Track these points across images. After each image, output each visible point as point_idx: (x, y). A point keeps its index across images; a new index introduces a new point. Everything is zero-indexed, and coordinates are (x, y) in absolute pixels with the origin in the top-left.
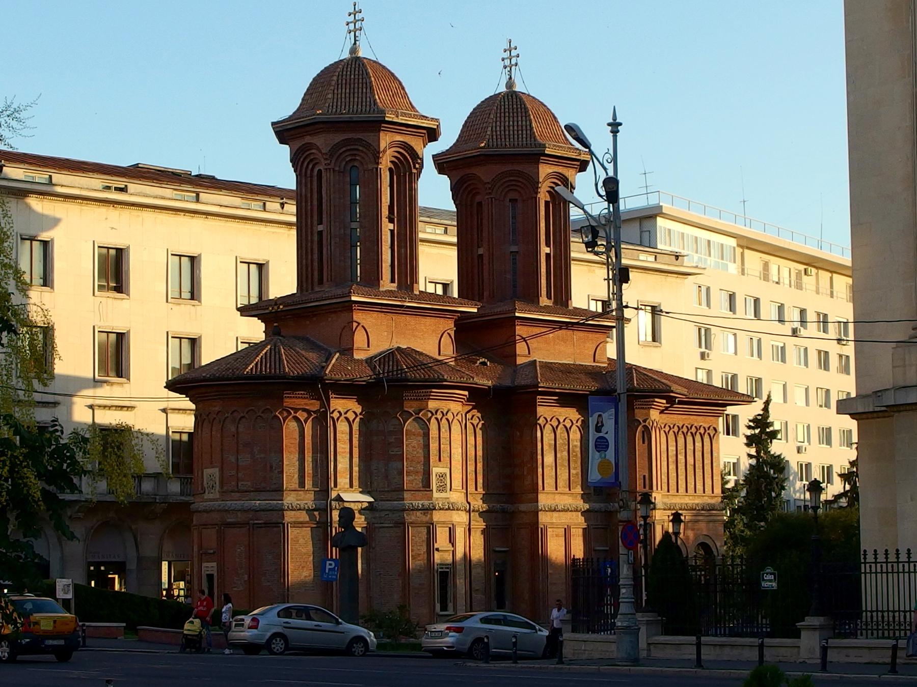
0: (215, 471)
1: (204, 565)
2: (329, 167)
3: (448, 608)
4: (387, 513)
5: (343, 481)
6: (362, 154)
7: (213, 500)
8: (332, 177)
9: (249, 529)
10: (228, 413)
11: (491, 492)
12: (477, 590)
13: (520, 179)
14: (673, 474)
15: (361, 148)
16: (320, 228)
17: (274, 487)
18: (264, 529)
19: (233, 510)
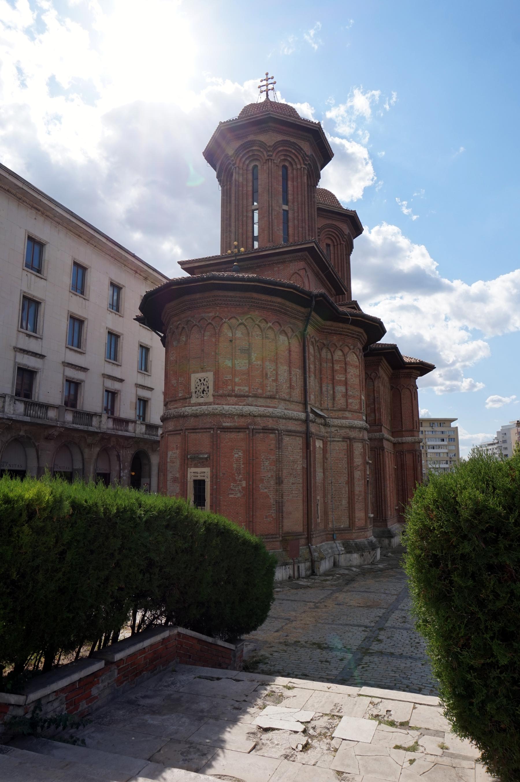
0: (210, 376)
2: (271, 158)
5: (312, 397)
7: (206, 404)
15: (293, 151)
17: (268, 394)
18: (261, 435)
19: (230, 414)
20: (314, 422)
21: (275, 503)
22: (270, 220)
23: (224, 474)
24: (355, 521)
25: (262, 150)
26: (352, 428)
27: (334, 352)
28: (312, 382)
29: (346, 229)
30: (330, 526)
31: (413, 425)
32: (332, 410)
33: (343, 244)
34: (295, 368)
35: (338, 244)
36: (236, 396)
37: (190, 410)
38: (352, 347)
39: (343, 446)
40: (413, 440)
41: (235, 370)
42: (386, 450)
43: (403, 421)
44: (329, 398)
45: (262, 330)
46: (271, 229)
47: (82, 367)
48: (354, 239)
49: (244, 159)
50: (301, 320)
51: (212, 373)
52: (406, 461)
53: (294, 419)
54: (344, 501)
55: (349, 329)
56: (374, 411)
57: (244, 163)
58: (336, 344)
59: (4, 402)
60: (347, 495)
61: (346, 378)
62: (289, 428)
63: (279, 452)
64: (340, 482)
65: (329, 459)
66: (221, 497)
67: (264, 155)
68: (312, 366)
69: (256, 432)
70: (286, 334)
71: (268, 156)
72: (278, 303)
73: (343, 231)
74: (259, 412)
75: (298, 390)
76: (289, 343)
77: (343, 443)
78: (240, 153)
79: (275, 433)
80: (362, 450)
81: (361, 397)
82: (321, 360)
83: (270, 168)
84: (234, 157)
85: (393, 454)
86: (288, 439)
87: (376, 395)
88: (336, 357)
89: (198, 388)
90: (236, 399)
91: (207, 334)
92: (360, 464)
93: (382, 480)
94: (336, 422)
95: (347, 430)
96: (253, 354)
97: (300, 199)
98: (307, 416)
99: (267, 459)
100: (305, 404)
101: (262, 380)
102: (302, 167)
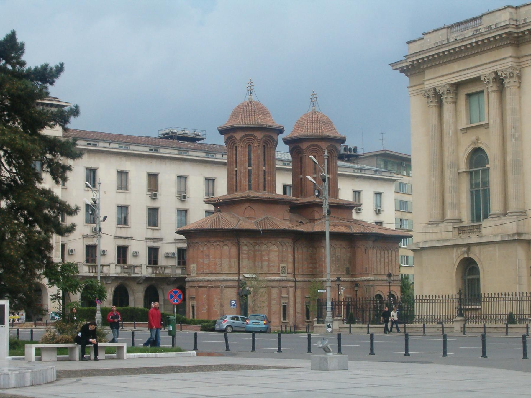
0: (195, 265)
1: (191, 302)
3: (286, 319)
5: (245, 270)
6: (253, 141)
11: (304, 273)
12: (299, 312)
13: (317, 148)
14: (379, 267)
15: (252, 138)
16: (236, 169)
17: (217, 272)
18: (214, 288)
28: (245, 263)
45: (214, 246)
59: (141, 269)
70: (228, 246)
77: (265, 288)
82: (255, 251)
91: (194, 249)
98: (239, 279)
100: (239, 274)
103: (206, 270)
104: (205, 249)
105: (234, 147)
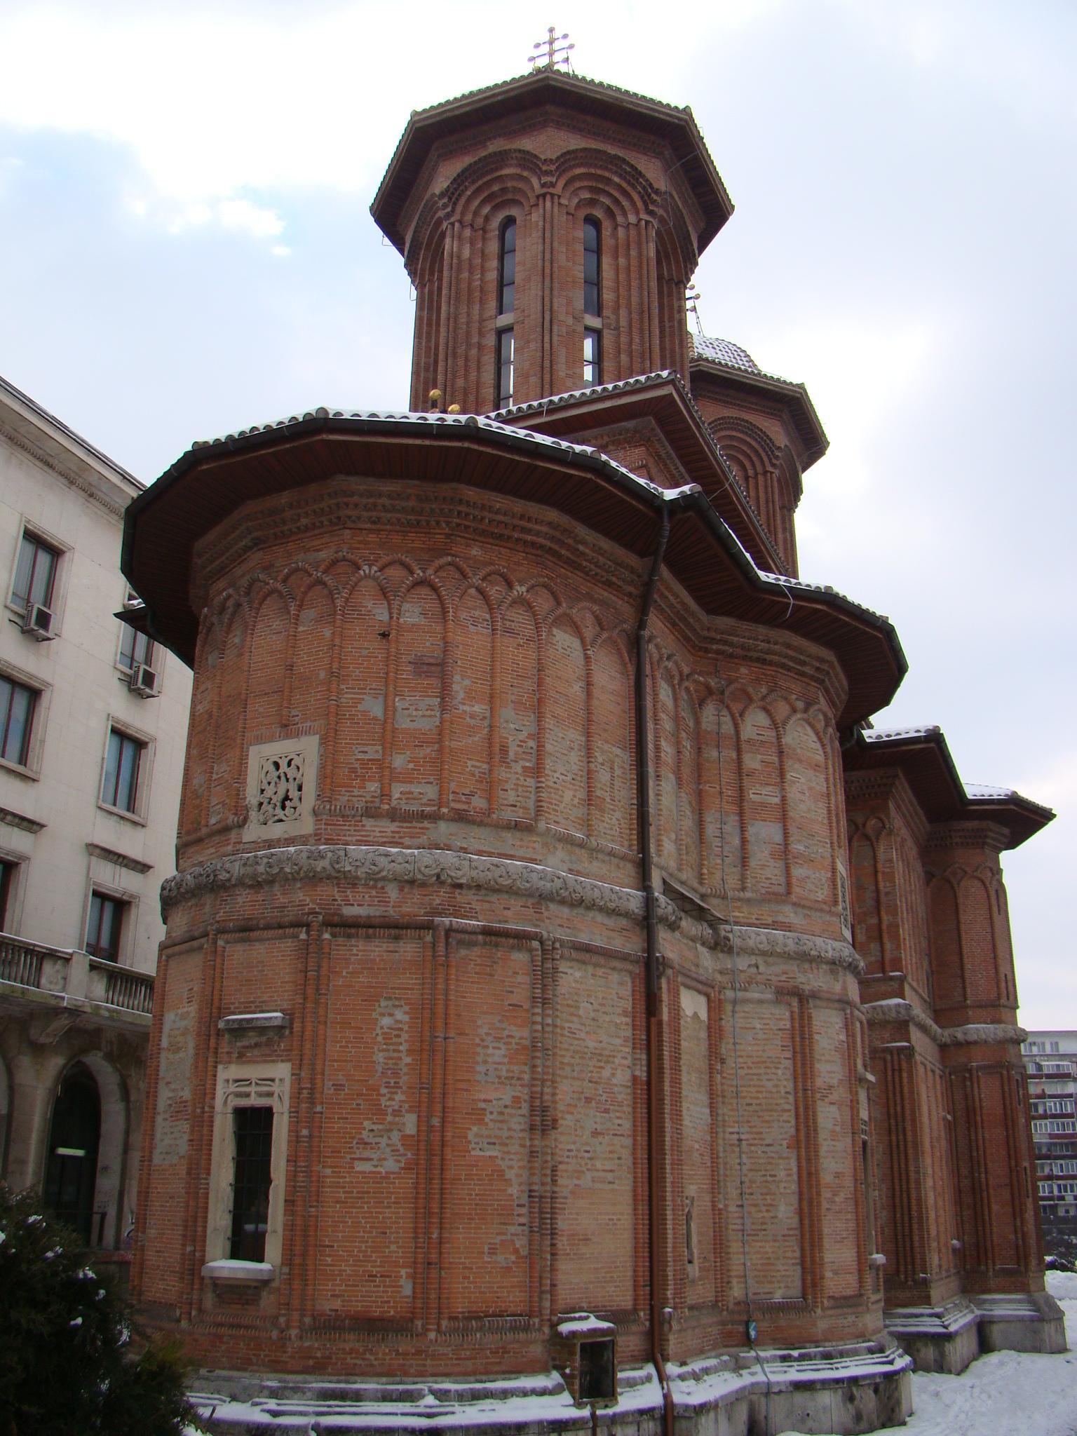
1: (227, 1073)
2: (551, 190)
4: (753, 960)
5: (669, 846)
8: (556, 209)
9: (434, 945)
10: (370, 566)
15: (616, 179)
16: (504, 320)
17: (509, 815)
20: (673, 927)
21: (524, 1199)
22: (547, 346)
23: (339, 1087)
24: (822, 1278)
25: (525, 174)
26: (806, 958)
27: (741, 715)
29: (778, 434)
30: (737, 1292)
31: (998, 987)
32: (740, 899)
33: (771, 473)
34: (607, 742)
35: (756, 474)
36: (393, 815)
37: (237, 864)
38: (800, 705)
39: (781, 1017)
40: (1000, 1034)
41: (394, 730)
42: (918, 1058)
43: (967, 975)
44: (728, 861)
46: (547, 370)
47: (23, 819)
48: (804, 469)
49: (476, 203)
50: (630, 595)
51: (317, 737)
52: (980, 1100)
53: (601, 909)
54: (782, 1208)
55: (788, 646)
56: (878, 934)
57: (476, 213)
58: (750, 690)
60: (794, 1187)
61: (784, 799)
62: (584, 938)
63: (544, 1016)
64: (767, 1142)
65: (730, 1062)
66: (328, 1171)
67: (532, 188)
68: (667, 749)
69: (461, 943)
70: (577, 630)
71: (543, 186)
72: (550, 524)
73: (771, 440)
74: (474, 873)
75: (618, 815)
76: (587, 658)
78: (466, 188)
79: (531, 950)
80: (843, 1037)
81: (833, 862)
82: (699, 739)
83: (548, 216)
84: (450, 199)
85: (941, 1077)
86: (578, 974)
87: (881, 885)
88: (748, 731)
89: (269, 792)
90: (394, 827)
91: (309, 614)
92: (835, 1082)
93: (910, 1151)
94: (753, 936)
95: (792, 967)
96: (457, 678)
97: (635, 300)
98: (649, 902)
99: (498, 1039)
101: (485, 766)
102: (640, 220)
103: (416, 789)
104: (412, 613)
105: (495, 223)
